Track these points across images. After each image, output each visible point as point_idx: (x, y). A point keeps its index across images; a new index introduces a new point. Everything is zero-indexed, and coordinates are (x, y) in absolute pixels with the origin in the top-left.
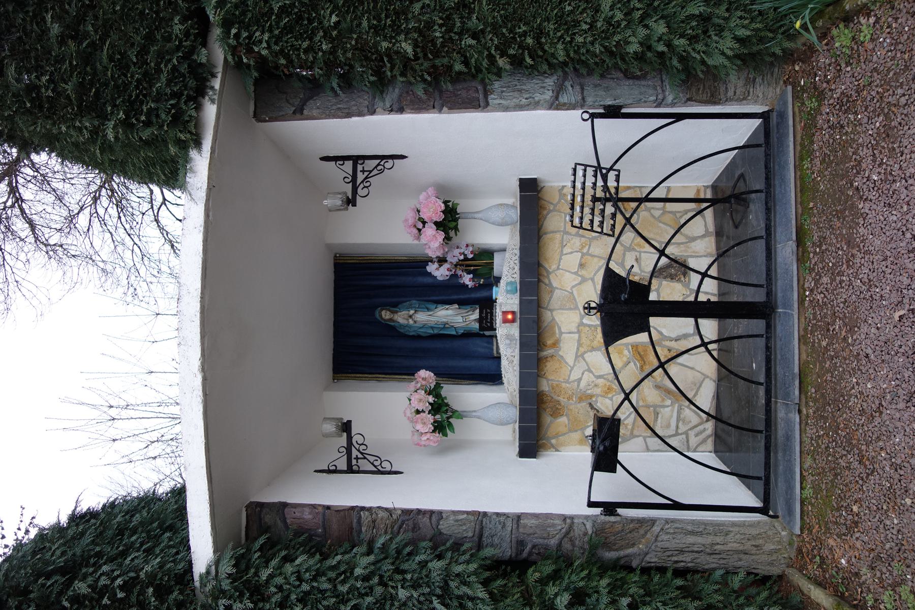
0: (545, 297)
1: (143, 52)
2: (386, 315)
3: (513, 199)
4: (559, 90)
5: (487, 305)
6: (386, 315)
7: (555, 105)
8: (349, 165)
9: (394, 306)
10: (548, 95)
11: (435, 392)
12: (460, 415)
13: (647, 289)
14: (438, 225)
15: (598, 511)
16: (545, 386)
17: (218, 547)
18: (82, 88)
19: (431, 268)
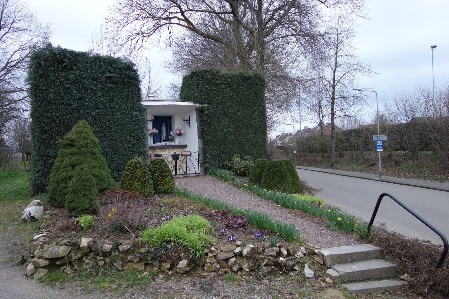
0: (170, 149)
1: (205, 97)
2: (164, 125)
4: (201, 148)
7: (199, 147)
10: (200, 146)
13: (178, 160)
14: (180, 133)
15: (150, 155)
16: (157, 150)
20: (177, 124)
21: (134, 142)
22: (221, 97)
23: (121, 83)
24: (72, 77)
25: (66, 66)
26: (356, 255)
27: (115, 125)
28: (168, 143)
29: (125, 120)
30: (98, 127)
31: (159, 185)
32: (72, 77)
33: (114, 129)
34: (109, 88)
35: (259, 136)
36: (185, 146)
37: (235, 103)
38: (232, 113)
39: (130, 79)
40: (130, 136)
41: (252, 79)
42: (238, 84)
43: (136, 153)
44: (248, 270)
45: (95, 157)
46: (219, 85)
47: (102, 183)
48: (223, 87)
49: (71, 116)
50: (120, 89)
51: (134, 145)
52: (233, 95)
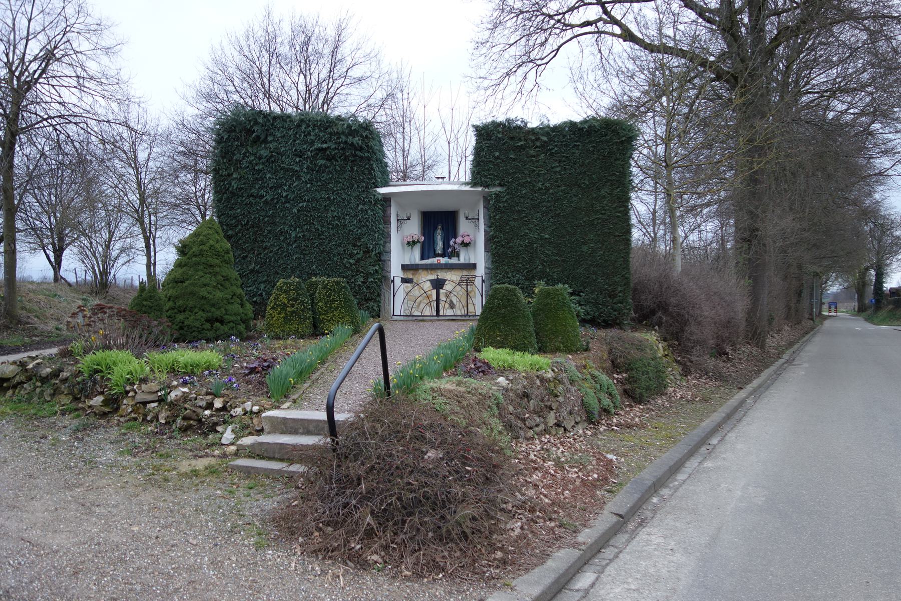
0: (444, 271)
2: (440, 227)
3: (472, 261)
5: (443, 255)
6: (440, 227)
7: (486, 268)
8: (477, 217)
9: (442, 229)
11: (418, 241)
12: (412, 248)
13: (442, 288)
16: (420, 271)
17: (383, 194)
18: (483, 161)
19: (453, 240)
20: (464, 227)
21: (359, 256)
22: (526, 172)
23: (340, 157)
24: (264, 153)
25: (258, 137)
26: (314, 424)
27: (328, 228)
28: (443, 260)
29: (344, 218)
30: (303, 231)
31: (322, 321)
32: (264, 153)
33: (327, 234)
34: (320, 167)
35: (612, 248)
36: (473, 266)
37: (556, 182)
38: (548, 201)
39: (356, 149)
40: (354, 245)
41: (599, 132)
42: (566, 146)
43: (362, 274)
44: (163, 421)
45: (211, 271)
46: (524, 149)
47: (213, 309)
48: (532, 152)
49: (263, 213)
50: (338, 168)
51: (358, 260)
52: (553, 168)
